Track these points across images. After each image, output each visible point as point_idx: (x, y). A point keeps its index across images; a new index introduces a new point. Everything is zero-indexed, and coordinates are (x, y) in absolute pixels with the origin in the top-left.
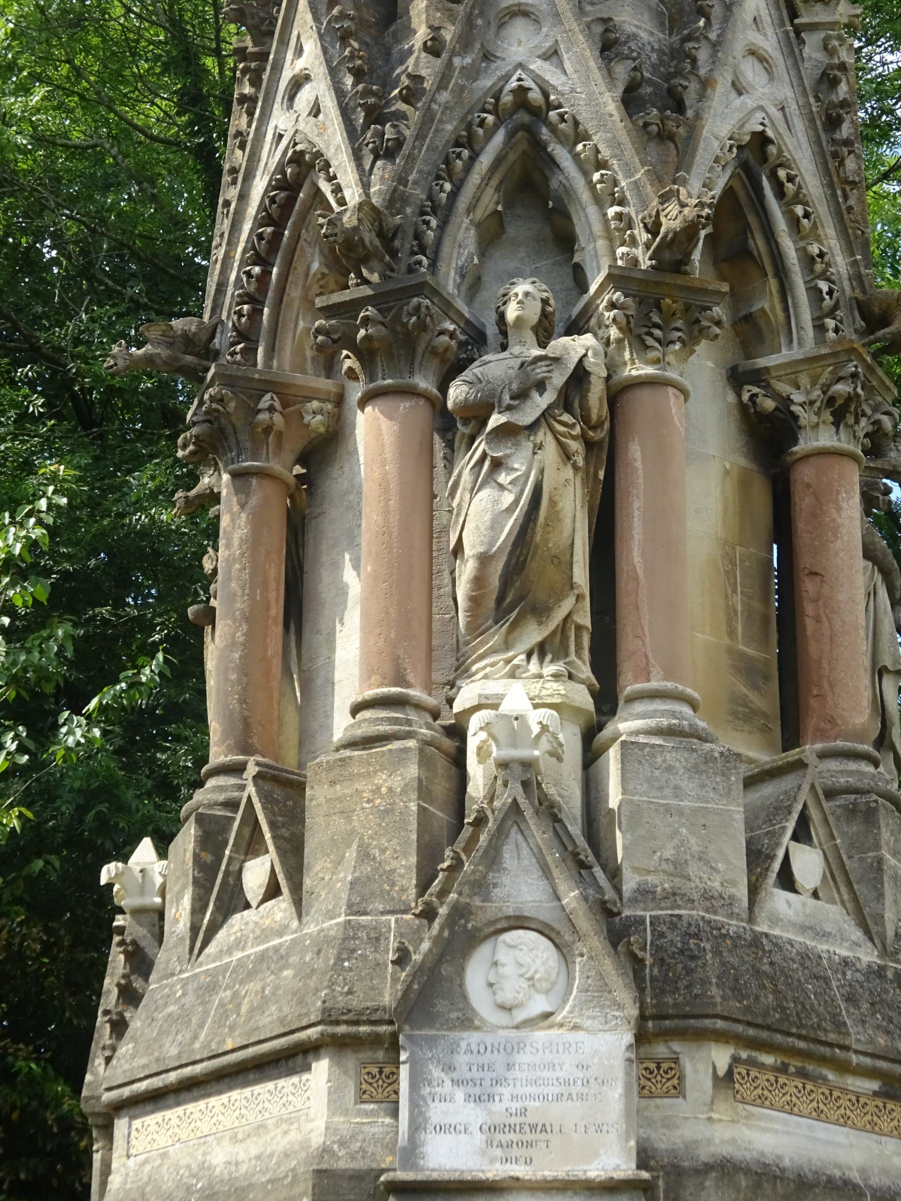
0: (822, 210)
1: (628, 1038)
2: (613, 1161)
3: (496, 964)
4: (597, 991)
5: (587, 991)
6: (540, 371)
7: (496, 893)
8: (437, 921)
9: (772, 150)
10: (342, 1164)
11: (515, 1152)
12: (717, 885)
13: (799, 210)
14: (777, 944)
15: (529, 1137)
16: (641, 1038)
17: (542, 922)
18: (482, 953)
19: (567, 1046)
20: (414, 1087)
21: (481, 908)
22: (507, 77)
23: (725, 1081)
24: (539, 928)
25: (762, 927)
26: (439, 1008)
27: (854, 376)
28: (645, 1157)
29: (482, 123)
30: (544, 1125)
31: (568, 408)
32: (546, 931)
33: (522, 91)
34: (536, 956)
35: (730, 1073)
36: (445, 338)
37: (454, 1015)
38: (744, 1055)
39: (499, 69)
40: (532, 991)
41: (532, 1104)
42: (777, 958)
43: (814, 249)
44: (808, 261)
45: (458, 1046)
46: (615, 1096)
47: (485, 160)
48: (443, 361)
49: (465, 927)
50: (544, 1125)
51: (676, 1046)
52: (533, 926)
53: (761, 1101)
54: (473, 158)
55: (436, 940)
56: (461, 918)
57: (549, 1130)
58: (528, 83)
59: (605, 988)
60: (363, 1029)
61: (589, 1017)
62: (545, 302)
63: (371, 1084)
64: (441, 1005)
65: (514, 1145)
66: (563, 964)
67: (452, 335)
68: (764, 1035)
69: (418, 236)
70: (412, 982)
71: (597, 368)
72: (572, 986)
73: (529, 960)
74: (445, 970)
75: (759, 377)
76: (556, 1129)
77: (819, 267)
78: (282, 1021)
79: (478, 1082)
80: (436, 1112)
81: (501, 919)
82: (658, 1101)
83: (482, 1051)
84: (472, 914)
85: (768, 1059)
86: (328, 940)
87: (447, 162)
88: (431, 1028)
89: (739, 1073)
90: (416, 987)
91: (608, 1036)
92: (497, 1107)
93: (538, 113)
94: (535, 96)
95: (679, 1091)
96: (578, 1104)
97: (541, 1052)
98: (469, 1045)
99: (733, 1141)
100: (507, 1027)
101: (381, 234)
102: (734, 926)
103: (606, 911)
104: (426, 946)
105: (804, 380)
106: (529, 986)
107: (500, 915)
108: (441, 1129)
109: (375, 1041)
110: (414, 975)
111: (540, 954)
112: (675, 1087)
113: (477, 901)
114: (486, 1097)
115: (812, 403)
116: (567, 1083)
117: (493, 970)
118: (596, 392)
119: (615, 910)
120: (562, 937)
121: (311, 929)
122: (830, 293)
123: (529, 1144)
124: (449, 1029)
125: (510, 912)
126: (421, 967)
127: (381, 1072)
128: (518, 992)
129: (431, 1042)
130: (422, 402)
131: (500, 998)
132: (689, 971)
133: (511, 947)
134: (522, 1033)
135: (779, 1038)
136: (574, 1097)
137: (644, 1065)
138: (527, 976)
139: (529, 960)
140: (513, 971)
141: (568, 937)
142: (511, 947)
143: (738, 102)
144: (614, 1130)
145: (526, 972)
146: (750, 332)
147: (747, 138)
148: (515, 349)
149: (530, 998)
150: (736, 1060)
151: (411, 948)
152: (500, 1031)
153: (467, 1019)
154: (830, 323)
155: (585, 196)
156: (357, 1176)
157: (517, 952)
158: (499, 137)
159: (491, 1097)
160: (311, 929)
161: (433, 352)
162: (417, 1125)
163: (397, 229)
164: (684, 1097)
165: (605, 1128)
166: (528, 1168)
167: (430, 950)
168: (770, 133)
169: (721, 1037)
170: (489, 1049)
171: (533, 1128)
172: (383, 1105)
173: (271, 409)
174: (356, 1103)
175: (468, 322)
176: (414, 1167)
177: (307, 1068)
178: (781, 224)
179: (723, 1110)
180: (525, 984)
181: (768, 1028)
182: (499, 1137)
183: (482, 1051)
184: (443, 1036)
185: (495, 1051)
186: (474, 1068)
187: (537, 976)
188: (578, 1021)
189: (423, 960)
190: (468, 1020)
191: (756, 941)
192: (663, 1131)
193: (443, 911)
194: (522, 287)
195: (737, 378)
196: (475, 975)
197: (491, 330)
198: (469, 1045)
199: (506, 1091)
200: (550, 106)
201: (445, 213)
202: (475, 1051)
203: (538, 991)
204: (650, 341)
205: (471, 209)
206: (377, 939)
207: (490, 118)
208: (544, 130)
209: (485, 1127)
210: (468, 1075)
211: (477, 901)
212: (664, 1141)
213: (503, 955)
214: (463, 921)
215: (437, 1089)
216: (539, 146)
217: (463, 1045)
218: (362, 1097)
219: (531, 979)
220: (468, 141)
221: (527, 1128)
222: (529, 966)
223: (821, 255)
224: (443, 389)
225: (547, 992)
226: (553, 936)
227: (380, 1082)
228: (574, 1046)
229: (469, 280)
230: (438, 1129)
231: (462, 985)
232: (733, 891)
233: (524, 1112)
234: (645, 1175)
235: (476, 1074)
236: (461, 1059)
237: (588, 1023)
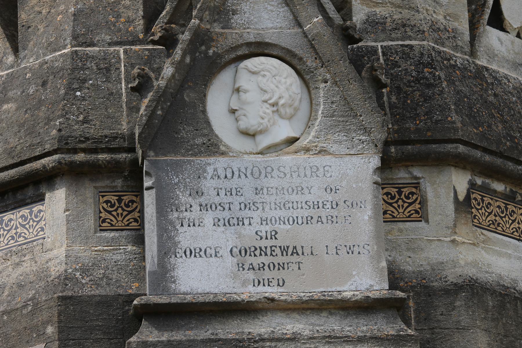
1: (375, 161)
2: (366, 280)
3: (238, 90)
4: (343, 116)
5: (333, 116)
7: (236, 19)
8: (180, 46)
10: (88, 291)
11: (267, 274)
12: (441, 18)
14: (497, 79)
15: (280, 259)
16: (387, 164)
17: (284, 48)
18: (224, 78)
19: (315, 170)
20: (162, 211)
21: (222, 34)
23: (464, 205)
24: (280, 54)
25: (482, 62)
26: (183, 134)
28: (395, 278)
30: (295, 248)
32: (287, 57)
34: (280, 82)
35: (468, 198)
37: (199, 141)
38: (479, 181)
40: (276, 117)
41: (281, 228)
42: (499, 90)
45: (205, 171)
46: (365, 217)
49: (206, 53)
50: (295, 248)
51: (417, 172)
52: (275, 53)
53: (494, 227)
55: (179, 66)
56: (201, 45)
57: (300, 252)
59: (350, 112)
60: (102, 157)
61: (335, 142)
63: (110, 212)
64: (185, 132)
65: (266, 267)
66: (305, 91)
68: (499, 161)
70: (156, 107)
72: (317, 111)
73: (272, 86)
74: (188, 96)
76: (307, 251)
78: (10, 152)
80: (186, 238)
81: (242, 45)
82: (401, 225)
83: (229, 175)
84: (213, 40)
85: (499, 187)
86: (55, 72)
88: (176, 154)
89: (475, 199)
90: (159, 112)
91: (354, 159)
92: (248, 231)
95: (422, 215)
96: (329, 226)
97: (288, 176)
98: (215, 170)
99: (475, 264)
100: (251, 153)
102: (460, 58)
103: (348, 36)
104: (168, 71)
106: (273, 112)
107: (241, 41)
108: (191, 253)
109: (113, 169)
110: (158, 100)
111: (283, 80)
112: (417, 212)
113: (217, 29)
114: (235, 221)
116: (316, 206)
117: (235, 96)
119: (357, 37)
120: (304, 63)
121: (30, 62)
123: (282, 266)
124: (195, 155)
125: (252, 39)
126: (162, 96)
127: (120, 201)
128: (263, 118)
129: (177, 167)
131: (243, 124)
132: (427, 99)
133: (254, 73)
134: (270, 158)
135: (511, 166)
136: (324, 220)
137: (385, 191)
138: (271, 102)
139: (272, 86)
140: (256, 98)
141: (311, 63)
142: (254, 73)
144: (366, 252)
145: (270, 99)
149: (274, 124)
150: (472, 185)
151: (152, 75)
152: (246, 156)
153: (212, 145)
156: (105, 302)
157: (260, 78)
159: (240, 221)
160: (30, 62)
162: (167, 249)
164: (427, 221)
166: (281, 290)
167: (173, 76)
169: (461, 162)
170: (236, 173)
171: (284, 250)
172: (124, 233)
174: (96, 232)
176: (166, 291)
177: (40, 199)
179: (465, 233)
180: (269, 110)
181: (501, 155)
182: (250, 260)
183: (229, 175)
184: (189, 162)
185: (243, 176)
187: (282, 102)
188: (325, 145)
189: (166, 87)
190: (213, 147)
191: (480, 73)
192: (409, 254)
193: (185, 37)
196: (217, 102)
198: (215, 170)
199: (256, 215)
202: (222, 176)
203: (281, 117)
206: (107, 69)
210: (217, 200)
211: (217, 29)
212: (411, 264)
213: (244, 81)
214: (203, 48)
215: (185, 214)
217: (210, 170)
218: (102, 225)
219: (273, 105)
221: (278, 251)
222: (273, 92)
225: (290, 118)
226: (295, 62)
227: (120, 211)
228: (321, 170)
230: (188, 253)
231: (204, 112)
232: (456, 24)
233: (274, 235)
234: (400, 294)
235: (224, 199)
236: (209, 184)
237: (334, 148)
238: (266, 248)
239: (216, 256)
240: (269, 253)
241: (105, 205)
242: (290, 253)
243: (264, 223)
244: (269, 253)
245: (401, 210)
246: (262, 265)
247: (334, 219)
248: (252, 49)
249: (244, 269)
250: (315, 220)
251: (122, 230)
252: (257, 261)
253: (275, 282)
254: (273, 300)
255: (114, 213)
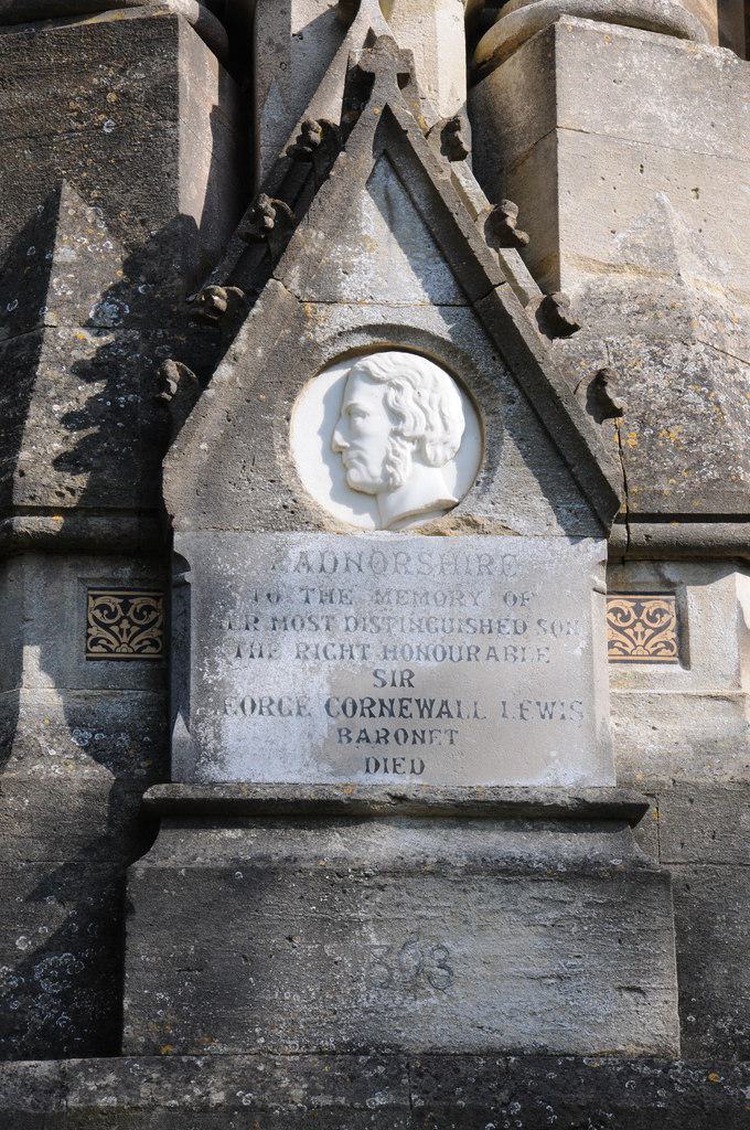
11: (390, 751)
12: (719, 295)
30: (445, 703)
52: (419, 348)
57: (454, 713)
63: (106, 627)
65: (391, 738)
76: (467, 710)
79: (322, 624)
82: (639, 668)
114: (337, 651)
119: (570, 321)
127: (126, 606)
136: (501, 655)
137: (612, 605)
144: (576, 717)
165: (558, 711)
166: (418, 781)
171: (425, 707)
172: (131, 666)
174: (80, 662)
186: (315, 598)
192: (653, 721)
202: (316, 567)
209: (336, 705)
210: (303, 609)
215: (246, 634)
221: (413, 708)
227: (125, 625)
230: (248, 706)
238: (392, 702)
239: (299, 713)
240: (396, 711)
241: (98, 614)
242: (435, 712)
243: (390, 655)
244: (396, 711)
245: (640, 642)
246: (383, 733)
247: (519, 654)
248: (383, 341)
249: (350, 740)
250: (482, 655)
251: (128, 660)
252: (373, 726)
253: (406, 766)
254: (401, 799)
255: (115, 629)
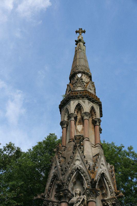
0: (110, 181)
6: (79, 199)
9: (104, 175)
13: (108, 181)
22: (76, 166)
27: (115, 201)
29: (73, 171)
31: (82, 204)
33: (78, 168)
36: (69, 196)
39: (76, 165)
43: (110, 186)
44: (109, 187)
47: (74, 175)
48: (69, 198)
54: (73, 175)
58: (79, 167)
62: (80, 191)
67: (70, 195)
69: (67, 184)
71: (85, 199)
75: (105, 201)
77: (110, 188)
87: (70, 175)
93: (79, 170)
94: (79, 168)
101: (62, 183)
105: (109, 201)
115: (110, 204)
118: (85, 202)
122: (112, 191)
130: (66, 203)
143: (101, 169)
146: (104, 195)
147: (102, 173)
148: (77, 197)
154: (112, 194)
155: (85, 180)
158: (75, 173)
161: (68, 197)
163: (64, 183)
168: (104, 173)
173: (51, 204)
175: (72, 194)
178: (106, 183)
194: (78, 189)
195: (103, 201)
197: (74, 195)
200: (81, 170)
201: (69, 181)
204: (91, 196)
205: (72, 181)
207: (74, 171)
208: (80, 172)
216: (80, 175)
220: (72, 173)
223: (111, 186)
224: (69, 202)
229: (72, 189)
